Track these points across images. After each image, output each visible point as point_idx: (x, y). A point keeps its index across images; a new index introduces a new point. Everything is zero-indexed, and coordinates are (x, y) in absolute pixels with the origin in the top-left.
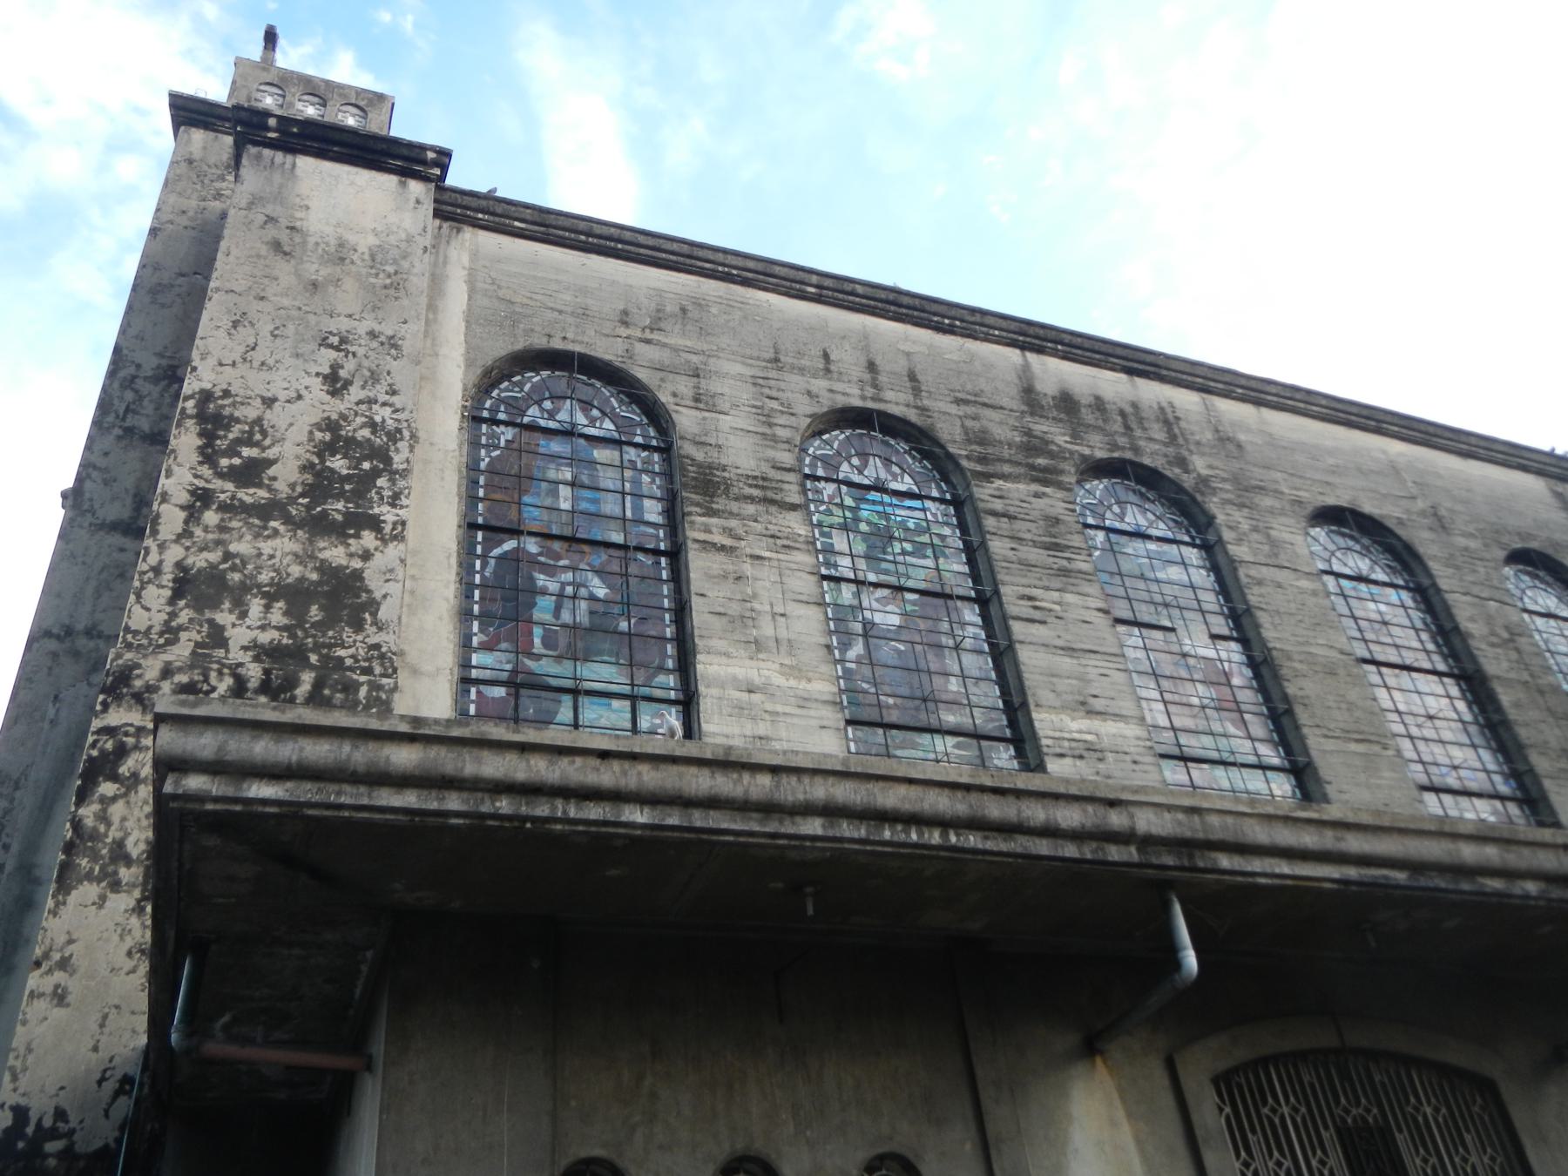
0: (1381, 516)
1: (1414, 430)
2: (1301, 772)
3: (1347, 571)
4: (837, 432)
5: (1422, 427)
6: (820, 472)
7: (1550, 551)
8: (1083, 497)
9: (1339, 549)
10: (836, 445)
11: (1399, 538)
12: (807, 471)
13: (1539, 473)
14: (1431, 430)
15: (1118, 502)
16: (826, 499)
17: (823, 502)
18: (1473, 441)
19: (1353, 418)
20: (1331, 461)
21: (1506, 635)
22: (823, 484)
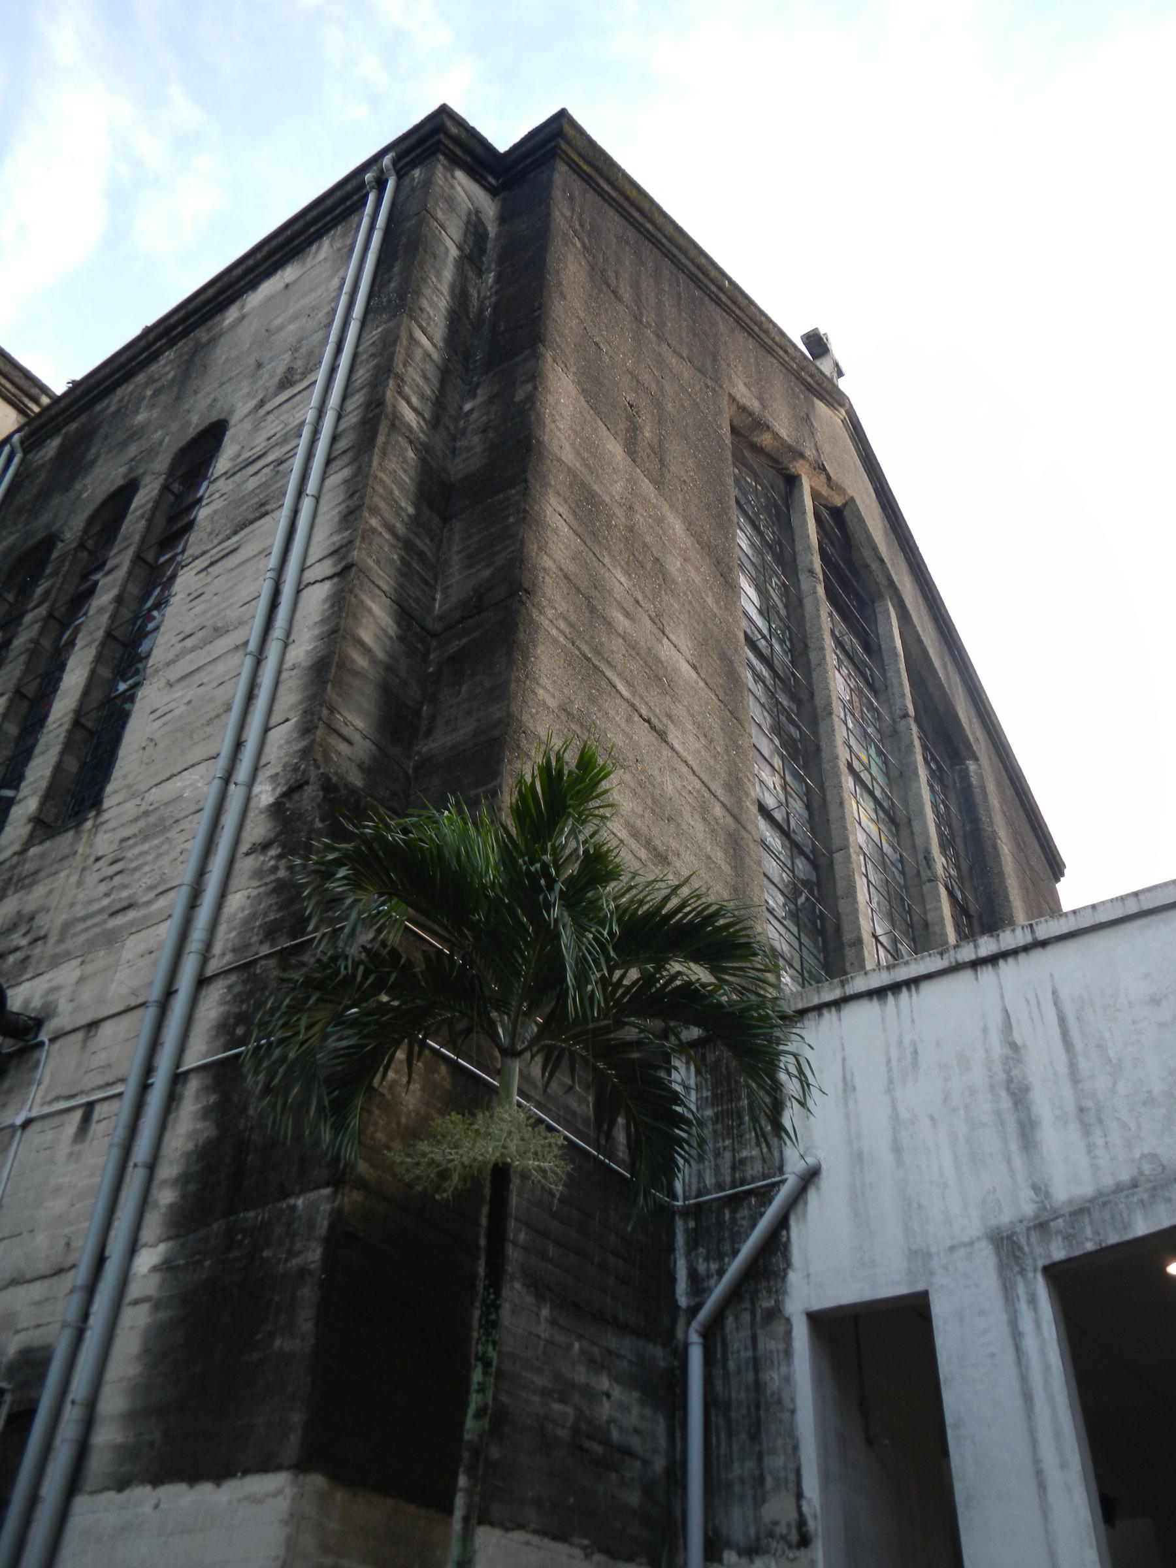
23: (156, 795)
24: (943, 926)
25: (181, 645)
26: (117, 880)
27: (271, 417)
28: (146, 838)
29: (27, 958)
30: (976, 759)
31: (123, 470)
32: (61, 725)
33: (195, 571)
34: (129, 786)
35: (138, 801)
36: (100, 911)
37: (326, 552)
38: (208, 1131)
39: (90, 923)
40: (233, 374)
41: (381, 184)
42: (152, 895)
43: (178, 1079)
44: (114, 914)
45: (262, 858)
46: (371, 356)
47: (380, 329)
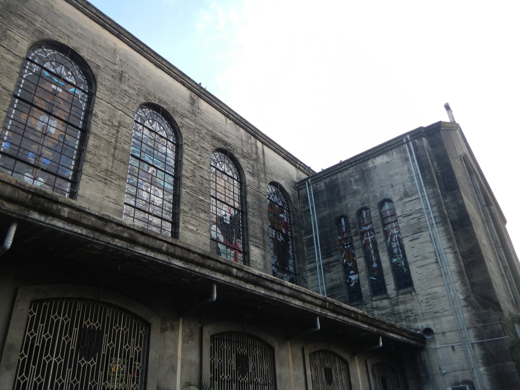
0: (88, 60)
1: (137, 45)
2: (175, 224)
3: (221, 169)
4: (51, 50)
5: (142, 46)
6: (36, 61)
7: (171, 112)
8: (140, 113)
9: (221, 161)
10: (48, 54)
11: (91, 71)
12: (30, 58)
13: (189, 89)
14: (145, 49)
15: (152, 120)
16: (34, 71)
17: (32, 72)
18: (164, 63)
19: (107, 25)
20: (79, 30)
21: (116, 124)
22: (35, 66)
23: (429, 291)
24: (504, 258)
25: (415, 259)
26: (430, 306)
27: (408, 204)
28: (433, 299)
29: (416, 318)
30: (492, 205)
31: (359, 202)
32: (388, 269)
33: (408, 240)
34: (421, 288)
35: (425, 291)
36: (430, 312)
37: (447, 247)
38: (483, 352)
39: (428, 314)
40: (384, 185)
41: (408, 142)
42: (442, 311)
43: (472, 344)
44: (434, 313)
45: (467, 308)
46: (433, 197)
47: (431, 190)
